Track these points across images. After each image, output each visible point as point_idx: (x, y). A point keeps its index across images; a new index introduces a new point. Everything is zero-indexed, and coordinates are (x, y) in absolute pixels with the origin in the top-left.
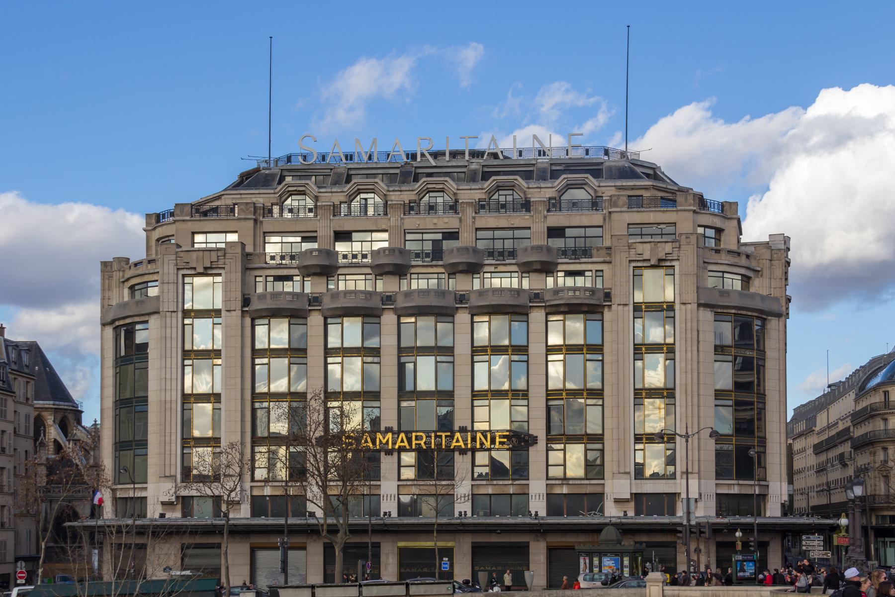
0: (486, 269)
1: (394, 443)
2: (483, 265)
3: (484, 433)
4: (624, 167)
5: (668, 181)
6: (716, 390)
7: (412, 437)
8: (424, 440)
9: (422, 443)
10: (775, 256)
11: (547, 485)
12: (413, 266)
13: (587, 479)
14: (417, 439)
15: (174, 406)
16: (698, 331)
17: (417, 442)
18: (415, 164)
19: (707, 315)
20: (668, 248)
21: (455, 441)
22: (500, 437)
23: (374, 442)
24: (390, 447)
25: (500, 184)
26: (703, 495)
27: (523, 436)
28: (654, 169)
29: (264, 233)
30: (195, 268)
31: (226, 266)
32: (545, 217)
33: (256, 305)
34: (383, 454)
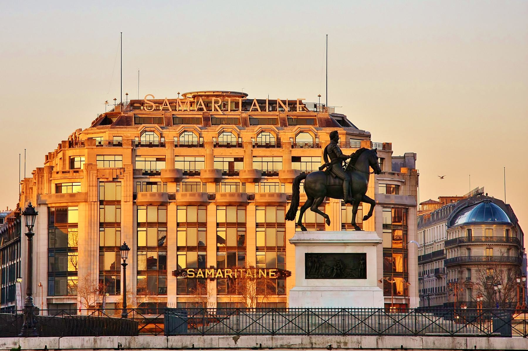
0: (262, 181)
1: (215, 275)
2: (260, 179)
4: (328, 119)
5: (351, 125)
6: (383, 248)
7: (224, 271)
12: (223, 179)
14: (227, 273)
15: (95, 254)
18: (211, 113)
23: (204, 274)
24: (213, 277)
27: (283, 272)
28: (343, 118)
29: (136, 155)
31: (124, 177)
32: (291, 151)
34: (208, 280)
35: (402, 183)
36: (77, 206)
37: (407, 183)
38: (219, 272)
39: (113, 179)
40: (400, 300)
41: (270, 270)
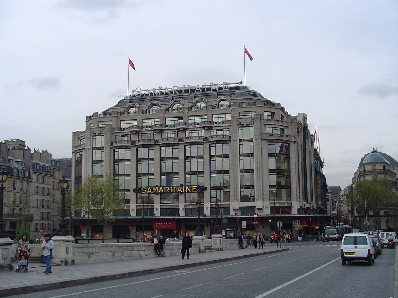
1: (158, 191)
3: (188, 187)
8: (168, 189)
9: (168, 190)
10: (293, 121)
11: (210, 204)
13: (224, 202)
14: (166, 189)
16: (262, 148)
17: (166, 190)
19: (265, 143)
20: (250, 120)
21: (179, 189)
22: (194, 188)
23: (152, 191)
25: (198, 100)
26: (265, 207)
28: (254, 93)
30: (95, 134)
32: (212, 111)
33: (115, 145)
35: (286, 127)
36: (82, 152)
37: (289, 127)
38: (180, 189)
39: (99, 133)
40: (283, 204)
41: (193, 187)
